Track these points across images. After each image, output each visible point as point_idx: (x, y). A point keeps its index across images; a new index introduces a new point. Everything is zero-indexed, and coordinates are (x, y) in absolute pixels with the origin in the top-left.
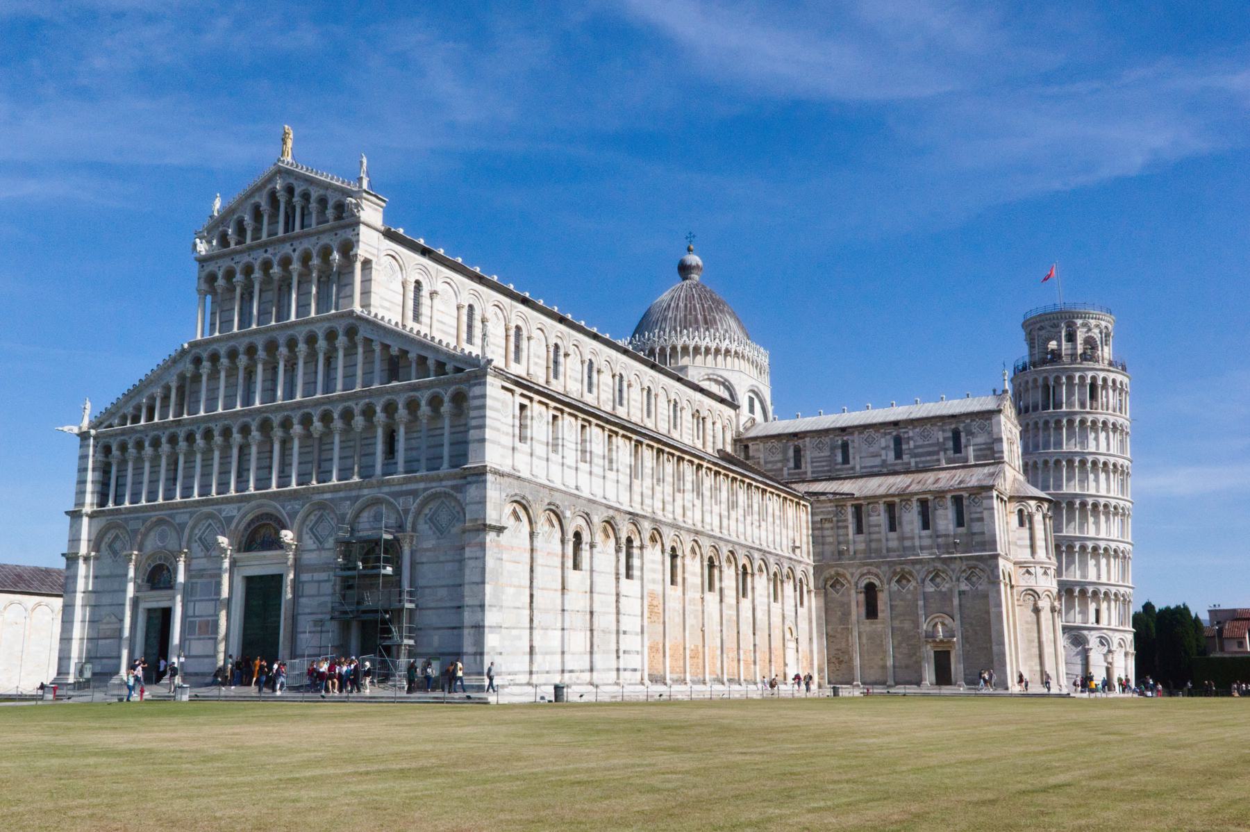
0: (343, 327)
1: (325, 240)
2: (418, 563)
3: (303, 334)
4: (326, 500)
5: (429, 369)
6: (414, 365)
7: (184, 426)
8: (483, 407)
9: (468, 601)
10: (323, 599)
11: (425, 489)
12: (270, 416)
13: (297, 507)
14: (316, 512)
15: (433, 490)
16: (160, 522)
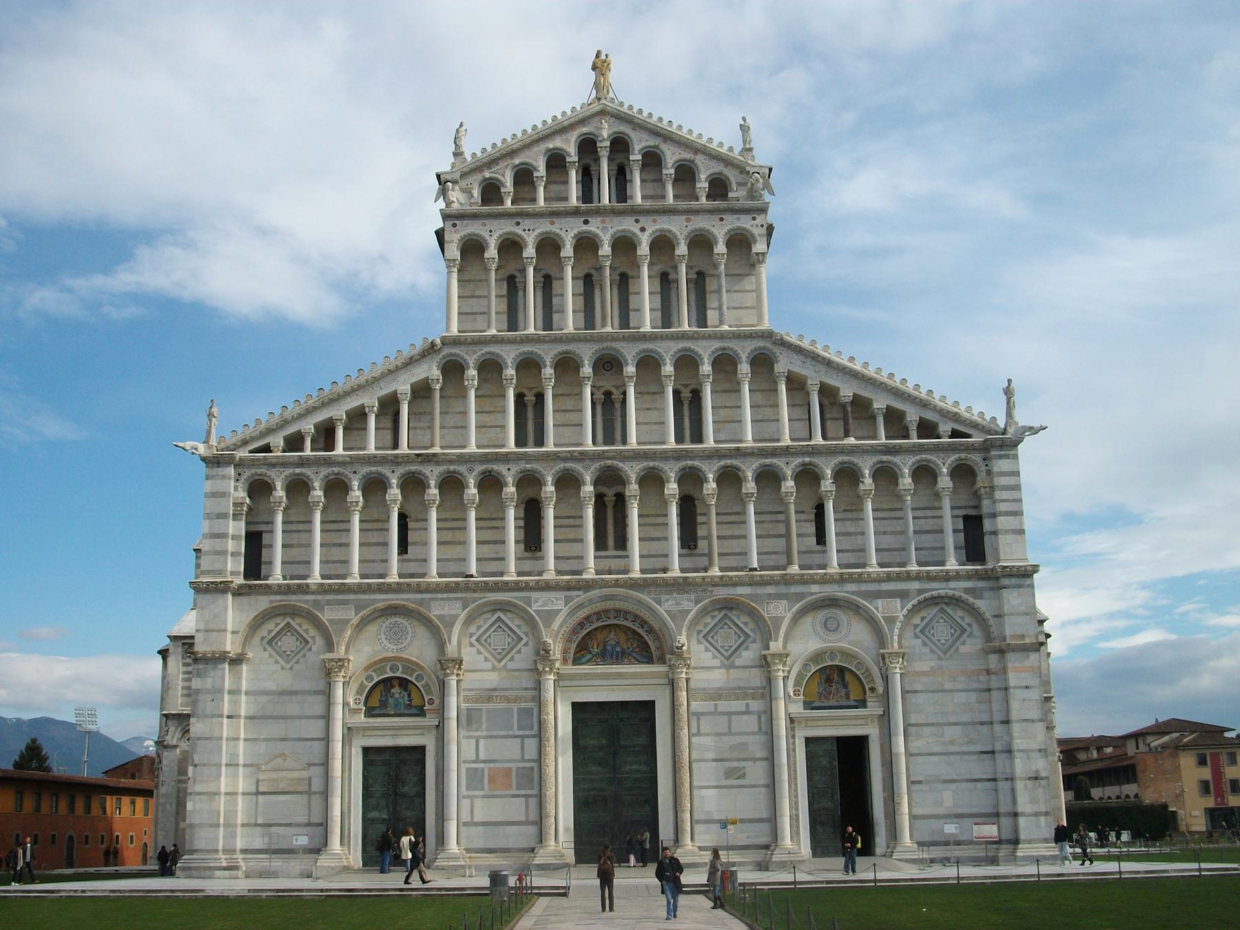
0: (748, 351)
1: (700, 223)
2: (907, 692)
3: (672, 353)
4: (741, 595)
5: (906, 429)
6: (880, 421)
7: (438, 463)
8: (1017, 487)
9: (1018, 743)
10: (738, 739)
11: (920, 592)
12: (620, 465)
13: (686, 602)
14: (716, 613)
15: (933, 593)
16: (392, 611)
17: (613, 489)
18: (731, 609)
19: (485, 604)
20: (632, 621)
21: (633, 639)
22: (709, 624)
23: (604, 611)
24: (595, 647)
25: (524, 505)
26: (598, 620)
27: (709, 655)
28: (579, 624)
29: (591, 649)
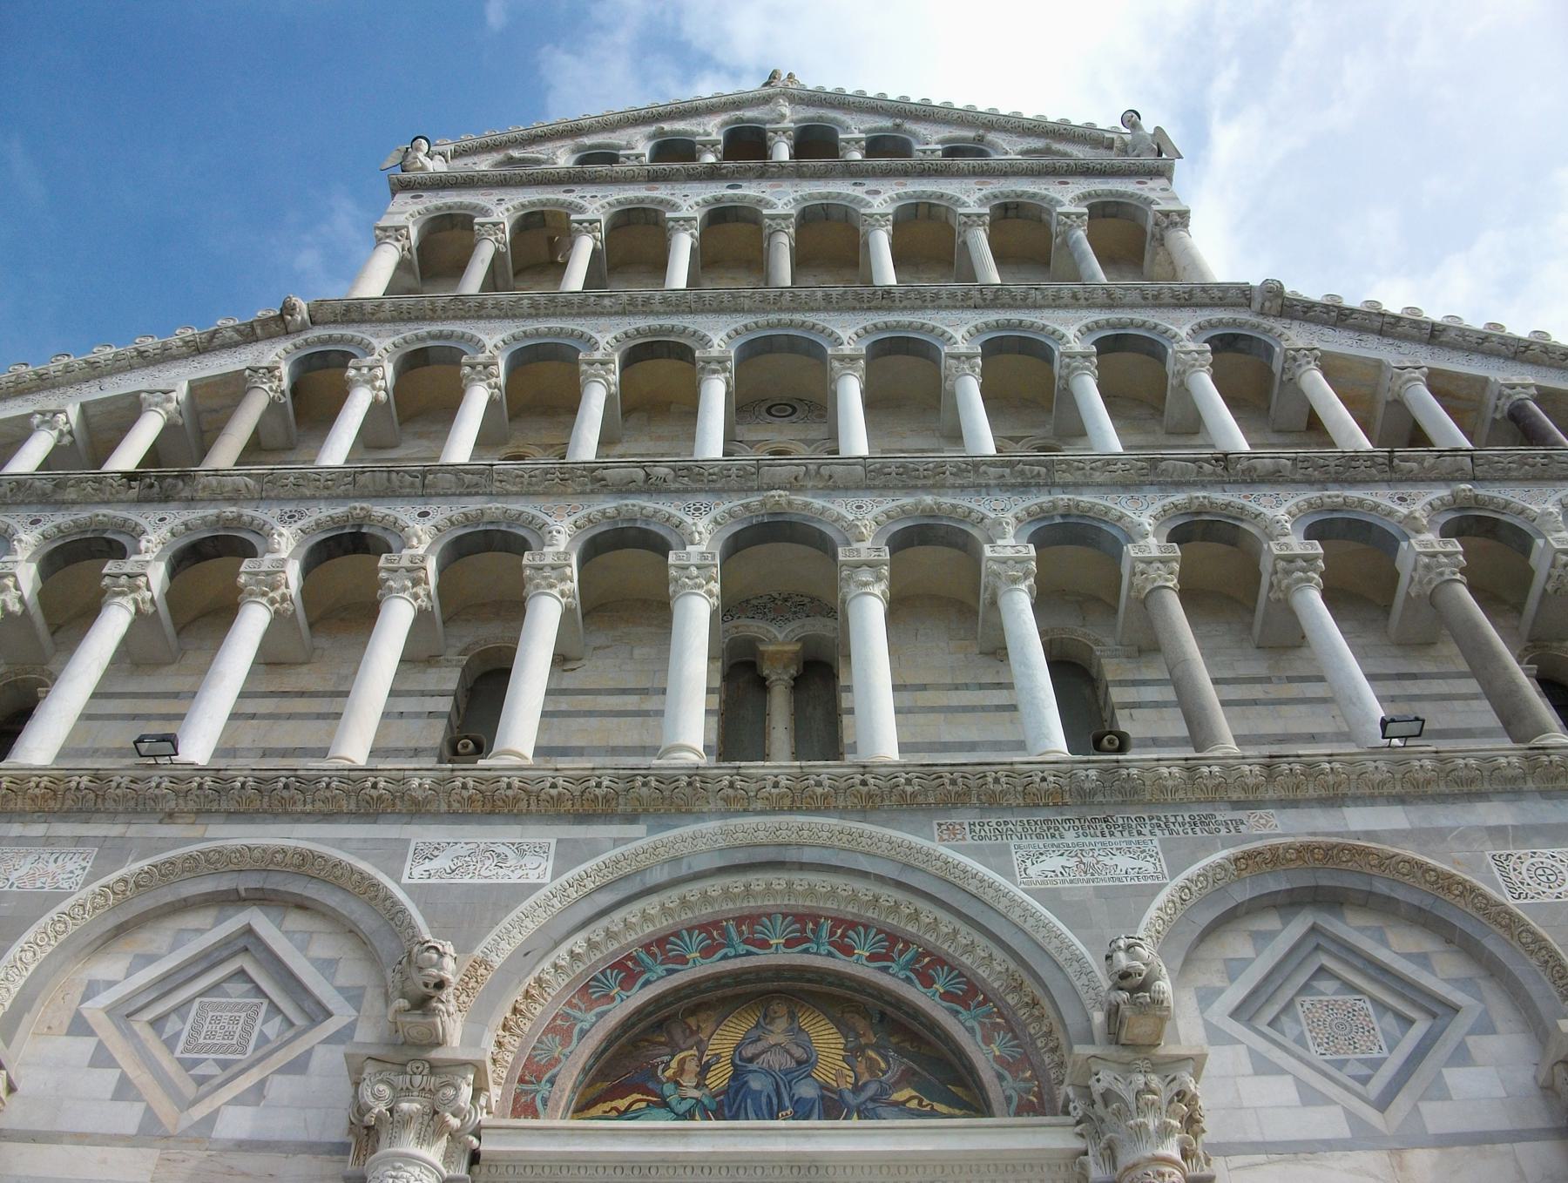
4: (1369, 835)
7: (191, 501)
13: (1124, 862)
14: (1270, 922)
17: (795, 624)
18: (1331, 899)
19: (194, 866)
20: (873, 958)
21: (877, 1048)
22: (1247, 962)
23: (740, 921)
24: (689, 1081)
25: (465, 659)
26: (707, 952)
27: (1281, 1090)
28: (619, 965)
29: (668, 1089)
